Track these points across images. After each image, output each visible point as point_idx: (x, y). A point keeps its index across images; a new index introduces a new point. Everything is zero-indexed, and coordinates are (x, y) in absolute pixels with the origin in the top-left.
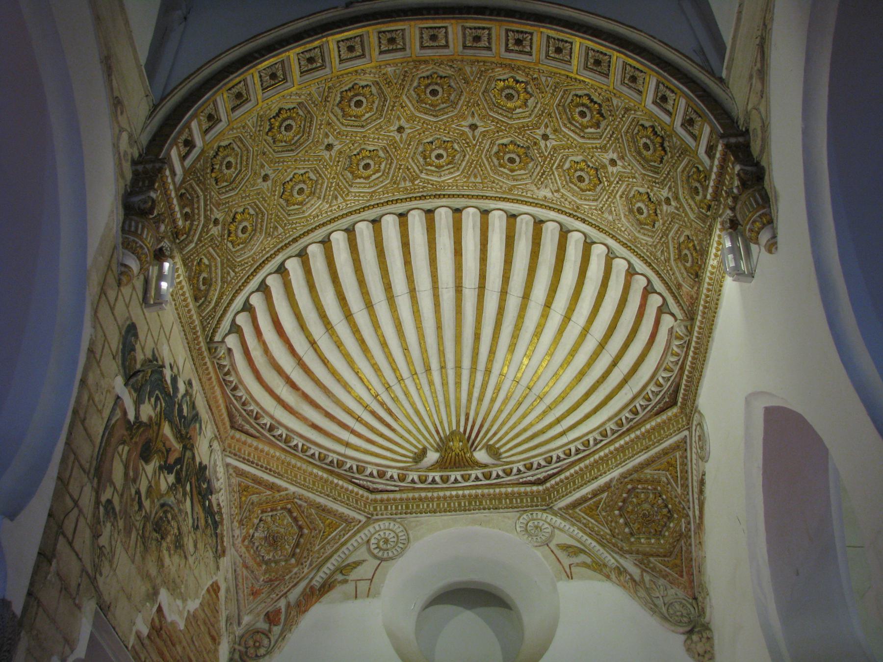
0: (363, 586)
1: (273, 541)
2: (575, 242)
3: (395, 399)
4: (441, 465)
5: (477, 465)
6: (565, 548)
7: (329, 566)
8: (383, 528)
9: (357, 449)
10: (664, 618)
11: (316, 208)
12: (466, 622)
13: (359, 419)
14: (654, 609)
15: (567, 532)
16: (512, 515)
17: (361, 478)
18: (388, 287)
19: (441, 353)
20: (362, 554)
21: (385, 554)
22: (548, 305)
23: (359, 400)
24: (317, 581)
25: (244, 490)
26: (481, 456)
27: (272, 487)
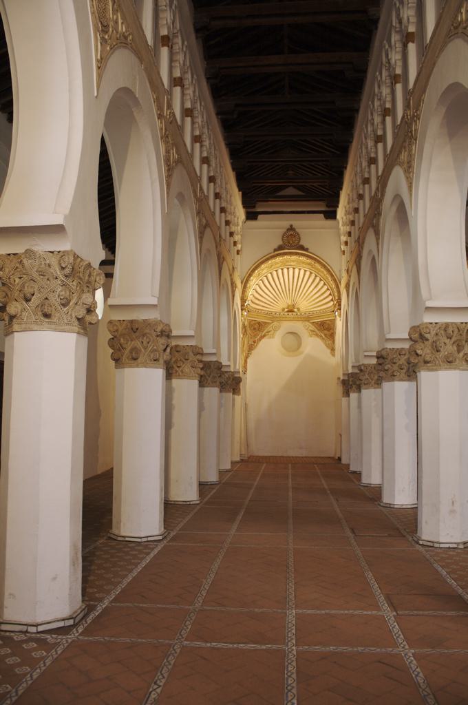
2: (318, 279)
4: (288, 311)
6: (311, 330)
7: (266, 331)
8: (275, 324)
12: (291, 336)
14: (326, 345)
15: (312, 328)
20: (271, 329)
26: (296, 310)
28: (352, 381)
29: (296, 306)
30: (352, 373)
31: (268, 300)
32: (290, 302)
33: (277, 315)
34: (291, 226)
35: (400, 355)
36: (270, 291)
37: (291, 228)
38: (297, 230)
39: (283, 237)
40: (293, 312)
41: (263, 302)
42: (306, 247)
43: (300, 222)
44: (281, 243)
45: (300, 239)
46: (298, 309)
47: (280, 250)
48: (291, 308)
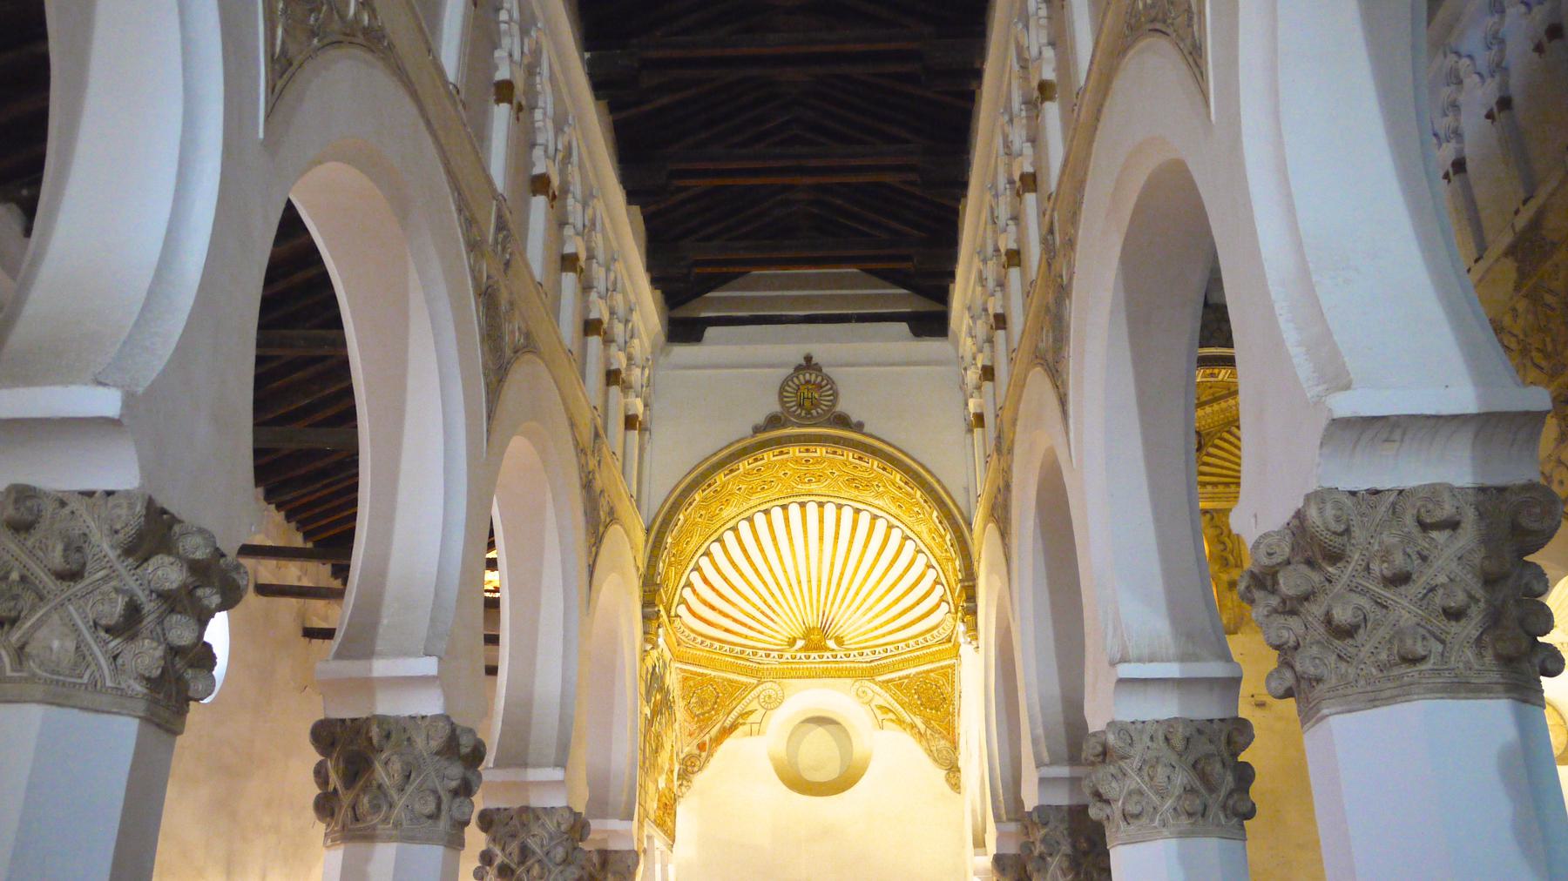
0: (755, 727)
1: (702, 703)
2: (896, 535)
3: (777, 602)
4: (805, 648)
5: (826, 649)
6: (881, 708)
8: (769, 687)
9: (752, 639)
10: (935, 760)
11: (728, 511)
12: (820, 732)
13: (753, 618)
14: (930, 753)
15: (884, 698)
16: (849, 681)
17: (756, 659)
18: (774, 539)
19: (809, 574)
21: (771, 704)
22: (880, 553)
23: (754, 606)
24: (728, 723)
25: (685, 679)
26: (831, 644)
27: (702, 675)
28: (1043, 841)
29: (831, 633)
30: (1038, 809)
31: (748, 615)
32: (812, 621)
33: (773, 662)
34: (808, 359)
35: (1424, 527)
36: (749, 583)
37: (809, 364)
38: (825, 370)
39: (782, 390)
40: (826, 649)
41: (726, 616)
42: (854, 419)
43: (834, 348)
44: (776, 408)
45: (835, 394)
46: (839, 641)
47: (771, 432)
48: (815, 637)
